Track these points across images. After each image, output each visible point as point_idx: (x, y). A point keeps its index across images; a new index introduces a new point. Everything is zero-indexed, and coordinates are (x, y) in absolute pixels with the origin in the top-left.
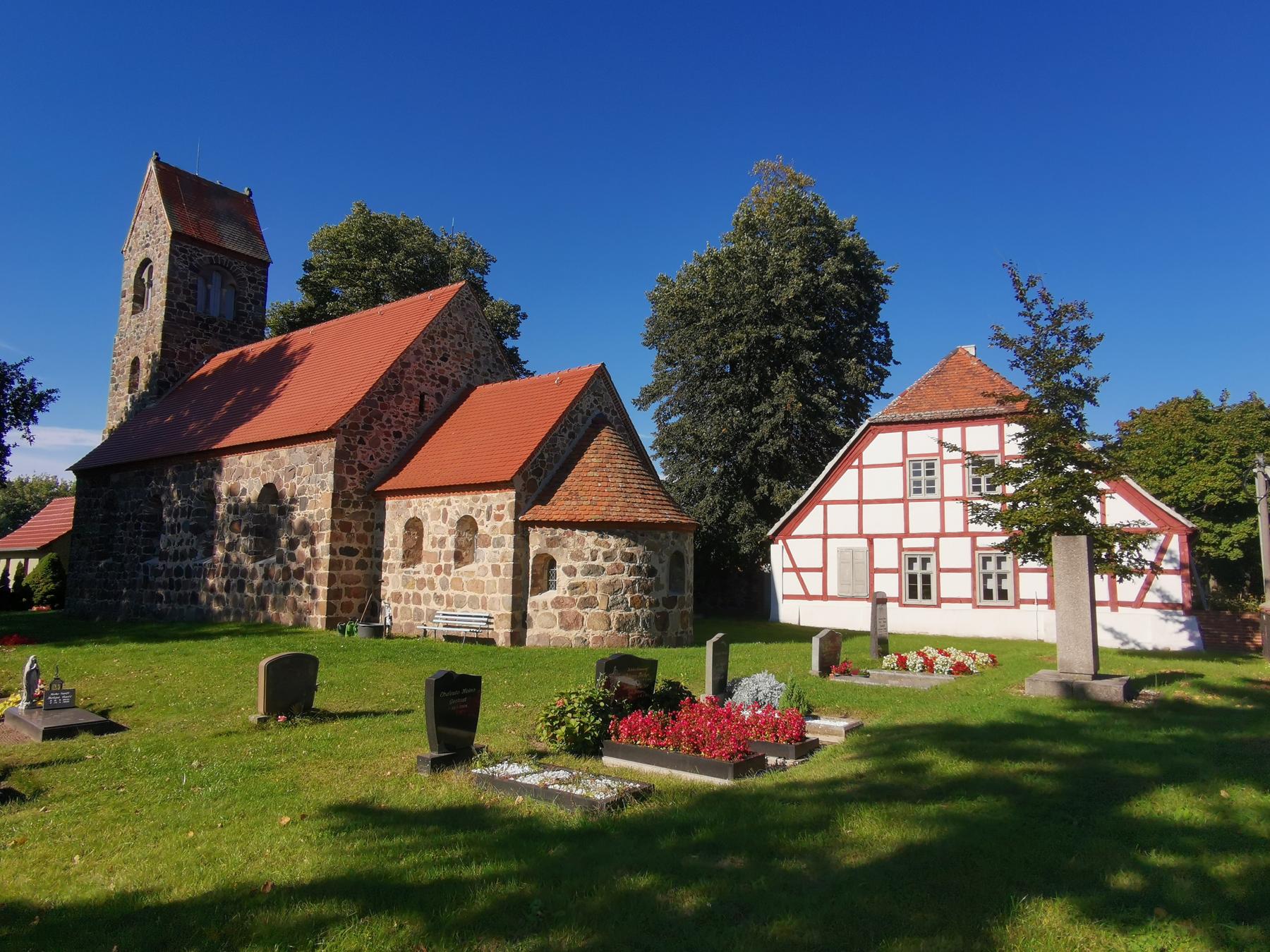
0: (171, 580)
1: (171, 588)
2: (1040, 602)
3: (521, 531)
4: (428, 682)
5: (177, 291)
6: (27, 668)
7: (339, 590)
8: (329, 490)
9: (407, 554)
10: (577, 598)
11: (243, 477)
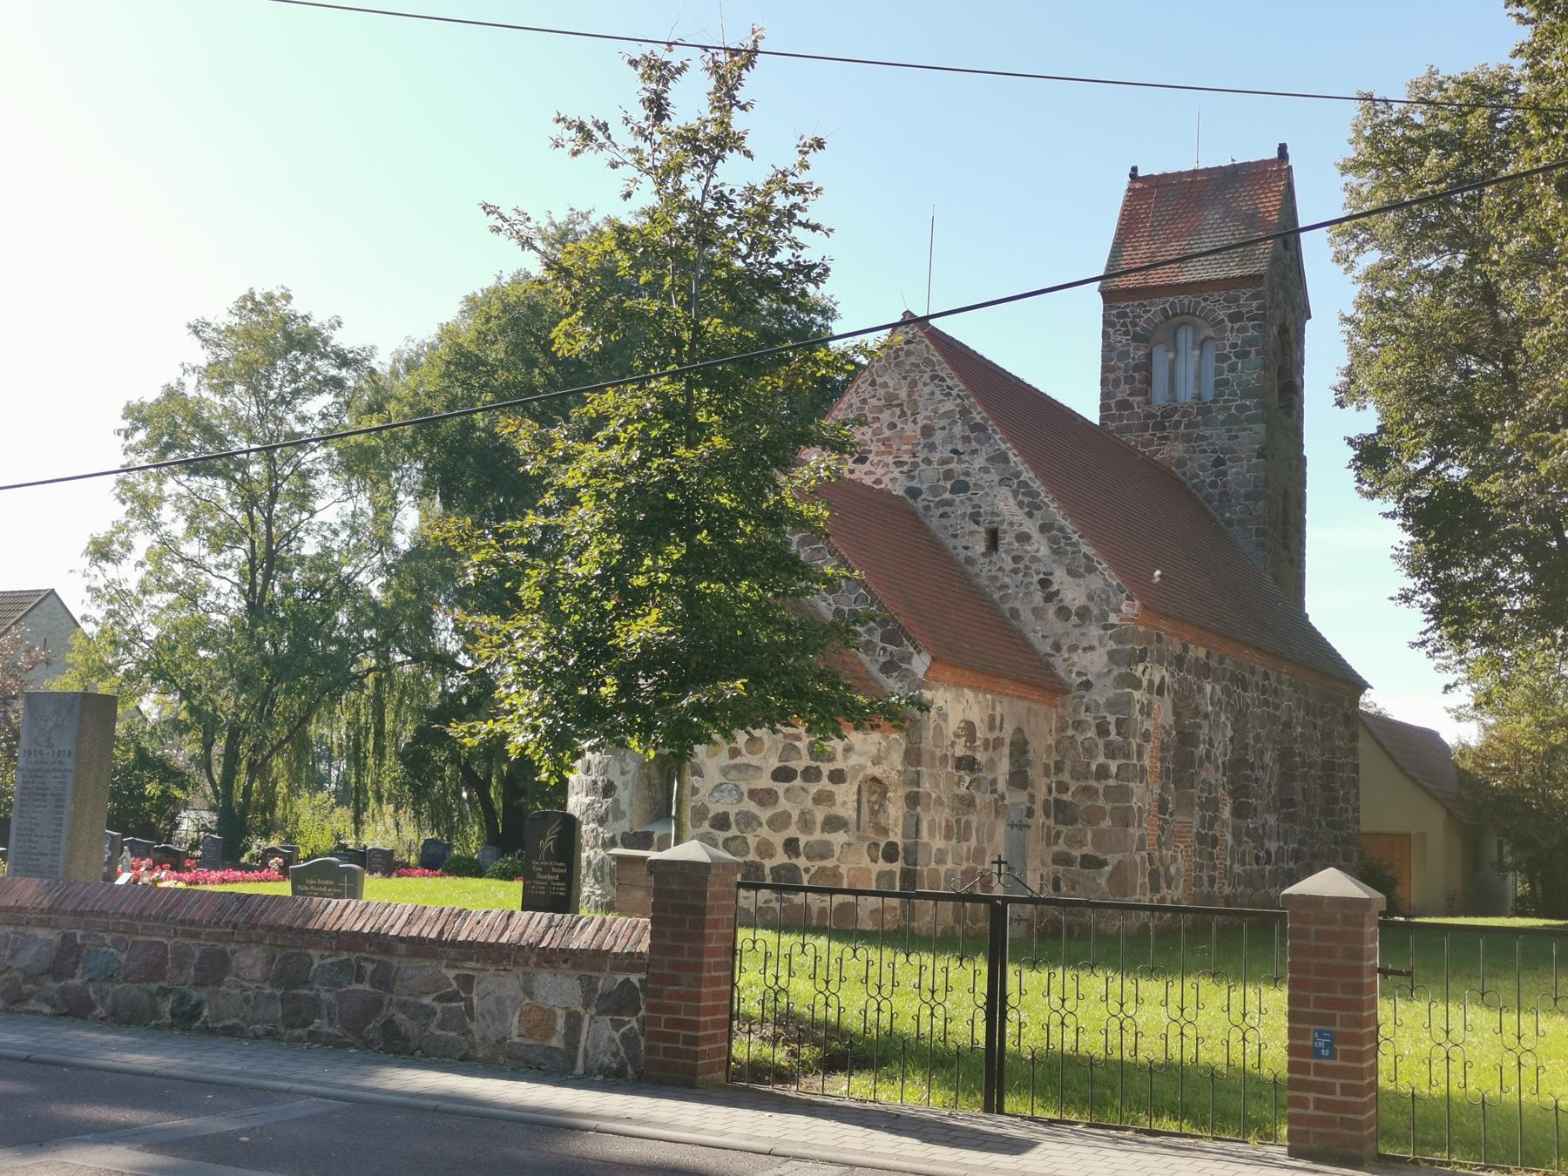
5: (1116, 383)
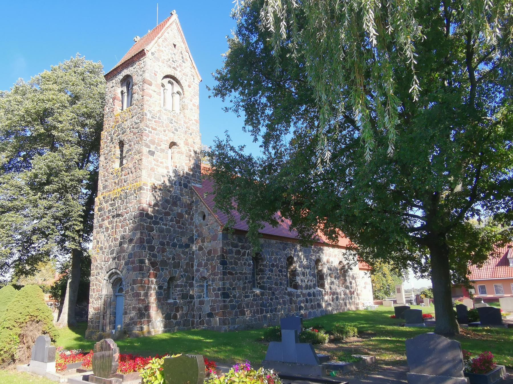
1: (307, 302)
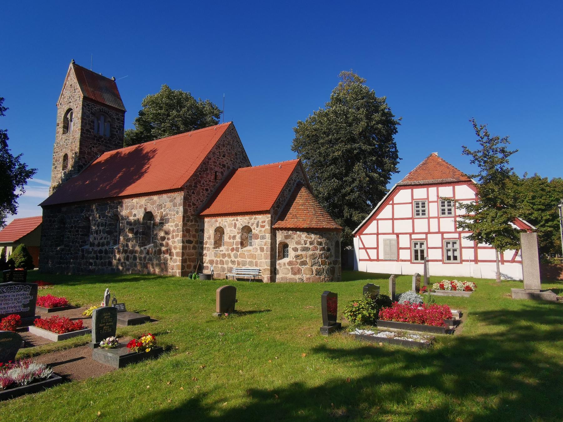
0: (97, 256)
1: (97, 259)
2: (471, 261)
3: (273, 232)
4: (322, 297)
6: (106, 294)
7: (186, 259)
8: (181, 214)
9: (215, 243)
10: (299, 261)
11: (133, 209)
